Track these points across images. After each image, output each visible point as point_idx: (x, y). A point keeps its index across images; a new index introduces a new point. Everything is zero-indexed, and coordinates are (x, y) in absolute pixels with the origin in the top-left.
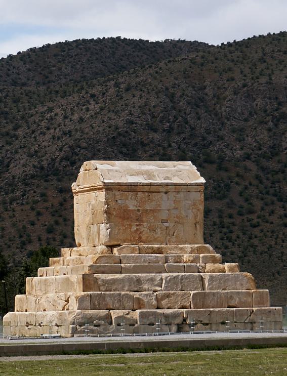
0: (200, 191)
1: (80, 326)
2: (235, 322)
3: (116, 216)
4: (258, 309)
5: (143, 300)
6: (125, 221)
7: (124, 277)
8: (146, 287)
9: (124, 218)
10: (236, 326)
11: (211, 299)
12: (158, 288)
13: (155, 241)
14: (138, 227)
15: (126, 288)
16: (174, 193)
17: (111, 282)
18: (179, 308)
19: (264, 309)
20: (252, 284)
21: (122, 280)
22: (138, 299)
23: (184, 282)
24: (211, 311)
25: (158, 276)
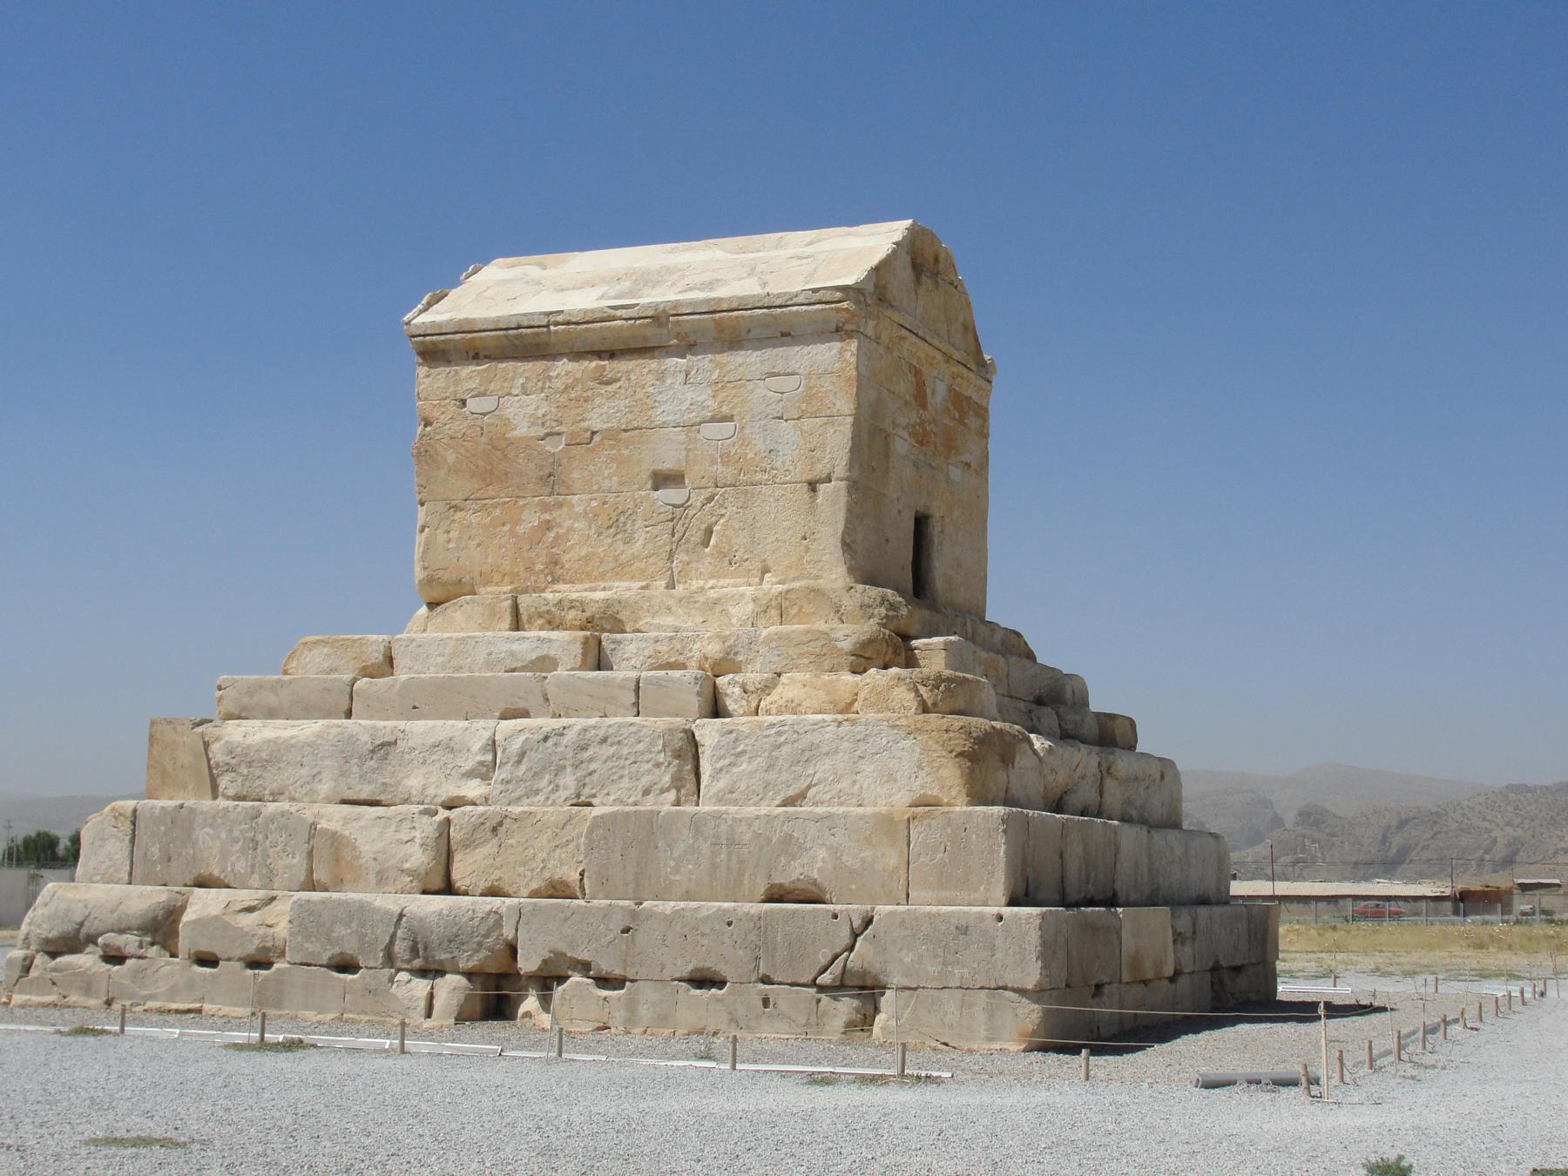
1: (54, 955)
2: (766, 980)
5: (354, 848)
6: (491, 491)
7: (319, 735)
10: (766, 1002)
11: (680, 848)
12: (473, 789)
13: (621, 569)
14: (547, 516)
15: (324, 788)
17: (264, 755)
18: (535, 894)
19: (930, 915)
20: (944, 772)
22: (336, 841)
23: (591, 760)
25: (482, 729)
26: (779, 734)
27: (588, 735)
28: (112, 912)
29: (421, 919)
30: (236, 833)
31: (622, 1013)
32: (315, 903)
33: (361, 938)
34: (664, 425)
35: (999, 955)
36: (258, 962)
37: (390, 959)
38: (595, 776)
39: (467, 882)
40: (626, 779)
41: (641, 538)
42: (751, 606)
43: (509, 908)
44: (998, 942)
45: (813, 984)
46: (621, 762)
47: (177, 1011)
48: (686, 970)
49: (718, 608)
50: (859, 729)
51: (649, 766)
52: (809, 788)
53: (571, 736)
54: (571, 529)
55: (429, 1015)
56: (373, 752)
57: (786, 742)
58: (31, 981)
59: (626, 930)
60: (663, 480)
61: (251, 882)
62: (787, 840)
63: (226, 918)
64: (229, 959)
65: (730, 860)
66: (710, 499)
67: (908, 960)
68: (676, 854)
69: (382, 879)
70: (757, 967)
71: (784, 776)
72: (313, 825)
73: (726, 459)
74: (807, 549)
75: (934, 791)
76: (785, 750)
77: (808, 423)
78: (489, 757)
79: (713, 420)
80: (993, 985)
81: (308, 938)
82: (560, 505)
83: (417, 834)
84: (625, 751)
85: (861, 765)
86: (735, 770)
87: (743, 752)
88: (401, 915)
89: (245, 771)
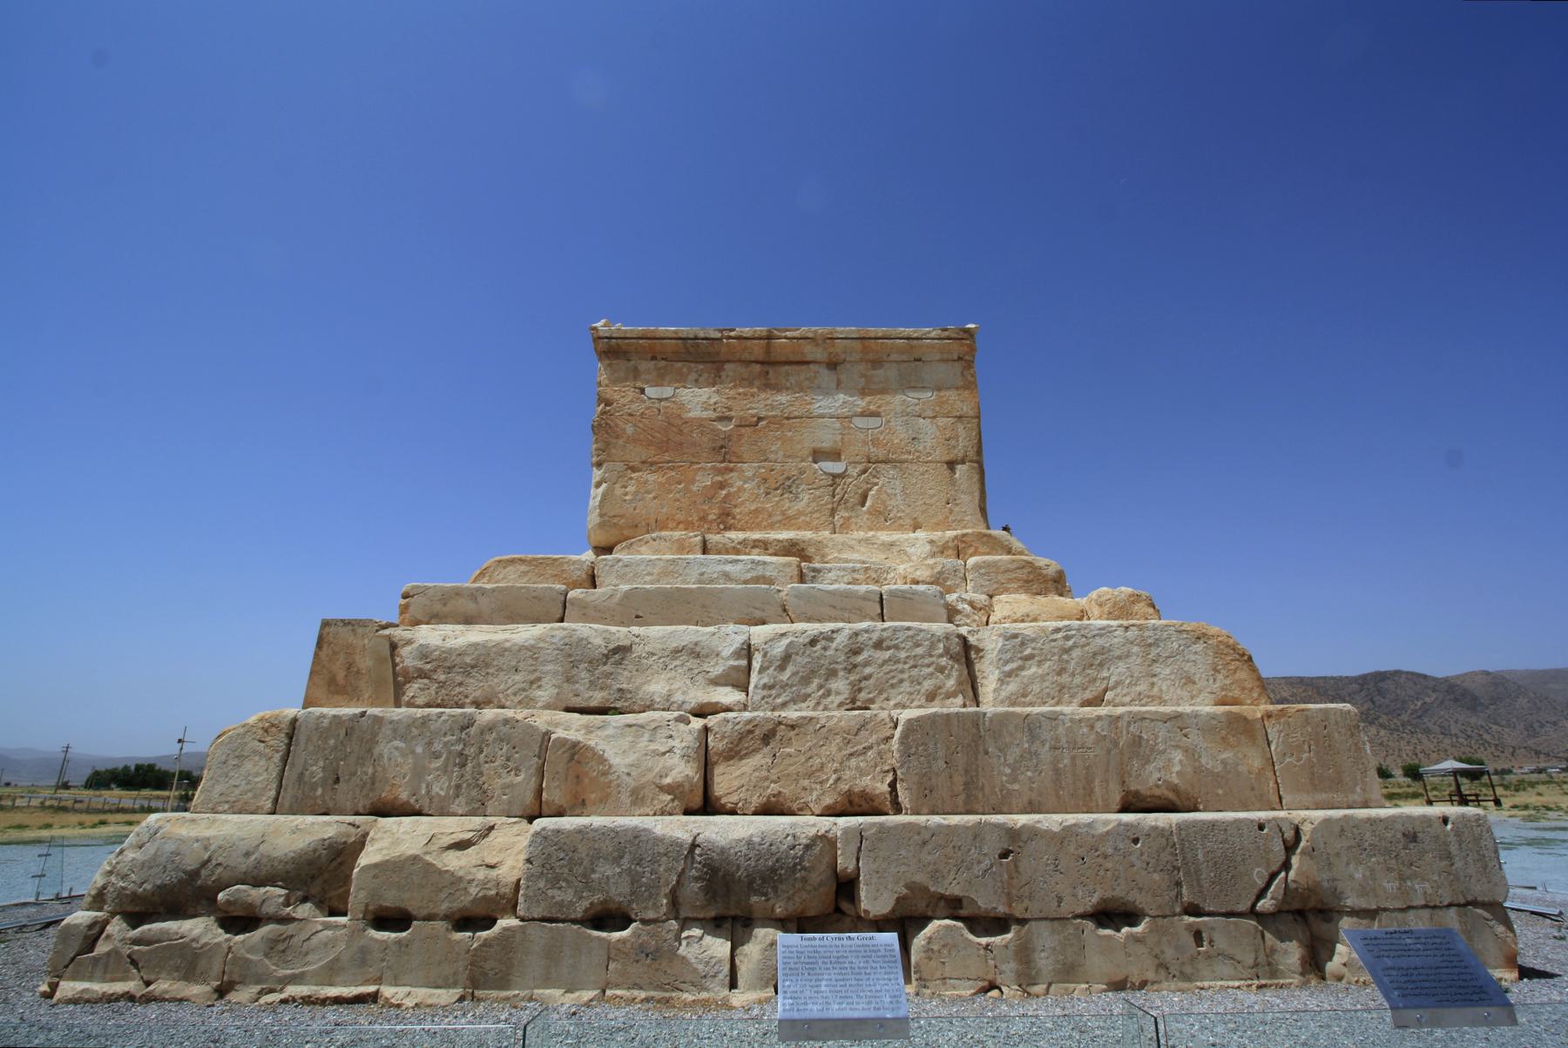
0: (960, 359)
1: (135, 919)
3: (634, 440)
4: (1327, 821)
5: (602, 760)
7: (540, 639)
8: (656, 687)
9: (664, 446)
10: (1198, 936)
11: (1013, 754)
13: (787, 522)
15: (544, 694)
16: (861, 367)
17: (468, 660)
21: (532, 651)
22: (575, 751)
23: (866, 664)
24: (1013, 834)
25: (731, 636)
26: (1067, 638)
27: (860, 639)
28: (247, 854)
29: (723, 851)
30: (437, 746)
31: (1013, 965)
32: (570, 834)
33: (635, 879)
34: (822, 416)
35: (1458, 864)
36: (469, 921)
37: (674, 903)
38: (872, 681)
39: (734, 798)
40: (906, 684)
41: (805, 497)
42: (928, 547)
43: (846, 831)
44: (1454, 849)
45: (1252, 913)
46: (900, 666)
47: (338, 1001)
48: (1090, 902)
49: (895, 549)
50: (1147, 634)
51: (931, 669)
52: (1106, 690)
53: (841, 639)
54: (740, 489)
55: (733, 985)
56: (607, 656)
57: (1075, 646)
58: (96, 960)
59: (1005, 855)
60: (818, 455)
61: (454, 808)
62: (1137, 741)
63: (428, 858)
64: (430, 918)
65: (1074, 764)
66: (864, 471)
67: (1358, 876)
68: (1011, 760)
69: (638, 799)
70: (1179, 894)
71: (1078, 680)
72: (547, 734)
73: (876, 442)
74: (951, 511)
75: (1236, 693)
76: (1076, 653)
77: (941, 421)
78: (744, 662)
79: (862, 415)
80: (1462, 901)
81: (554, 882)
82: (732, 470)
83: (676, 743)
84: (903, 655)
85: (1157, 669)
86: (1024, 673)
87: (1030, 657)
88: (694, 846)
89: (442, 677)
